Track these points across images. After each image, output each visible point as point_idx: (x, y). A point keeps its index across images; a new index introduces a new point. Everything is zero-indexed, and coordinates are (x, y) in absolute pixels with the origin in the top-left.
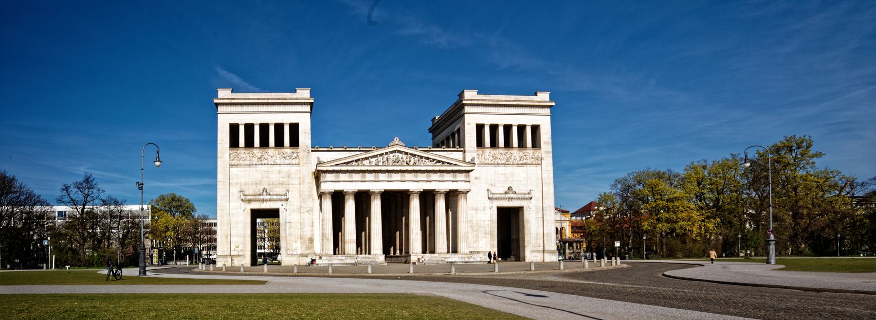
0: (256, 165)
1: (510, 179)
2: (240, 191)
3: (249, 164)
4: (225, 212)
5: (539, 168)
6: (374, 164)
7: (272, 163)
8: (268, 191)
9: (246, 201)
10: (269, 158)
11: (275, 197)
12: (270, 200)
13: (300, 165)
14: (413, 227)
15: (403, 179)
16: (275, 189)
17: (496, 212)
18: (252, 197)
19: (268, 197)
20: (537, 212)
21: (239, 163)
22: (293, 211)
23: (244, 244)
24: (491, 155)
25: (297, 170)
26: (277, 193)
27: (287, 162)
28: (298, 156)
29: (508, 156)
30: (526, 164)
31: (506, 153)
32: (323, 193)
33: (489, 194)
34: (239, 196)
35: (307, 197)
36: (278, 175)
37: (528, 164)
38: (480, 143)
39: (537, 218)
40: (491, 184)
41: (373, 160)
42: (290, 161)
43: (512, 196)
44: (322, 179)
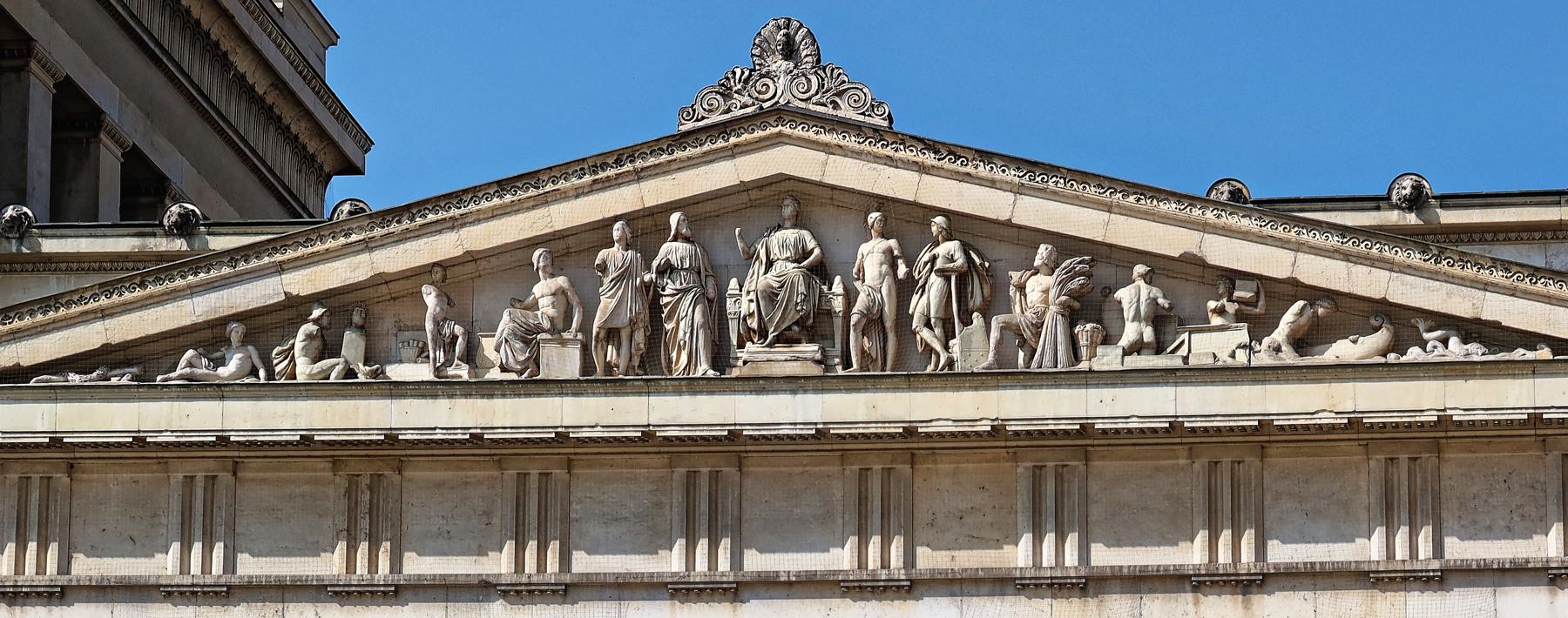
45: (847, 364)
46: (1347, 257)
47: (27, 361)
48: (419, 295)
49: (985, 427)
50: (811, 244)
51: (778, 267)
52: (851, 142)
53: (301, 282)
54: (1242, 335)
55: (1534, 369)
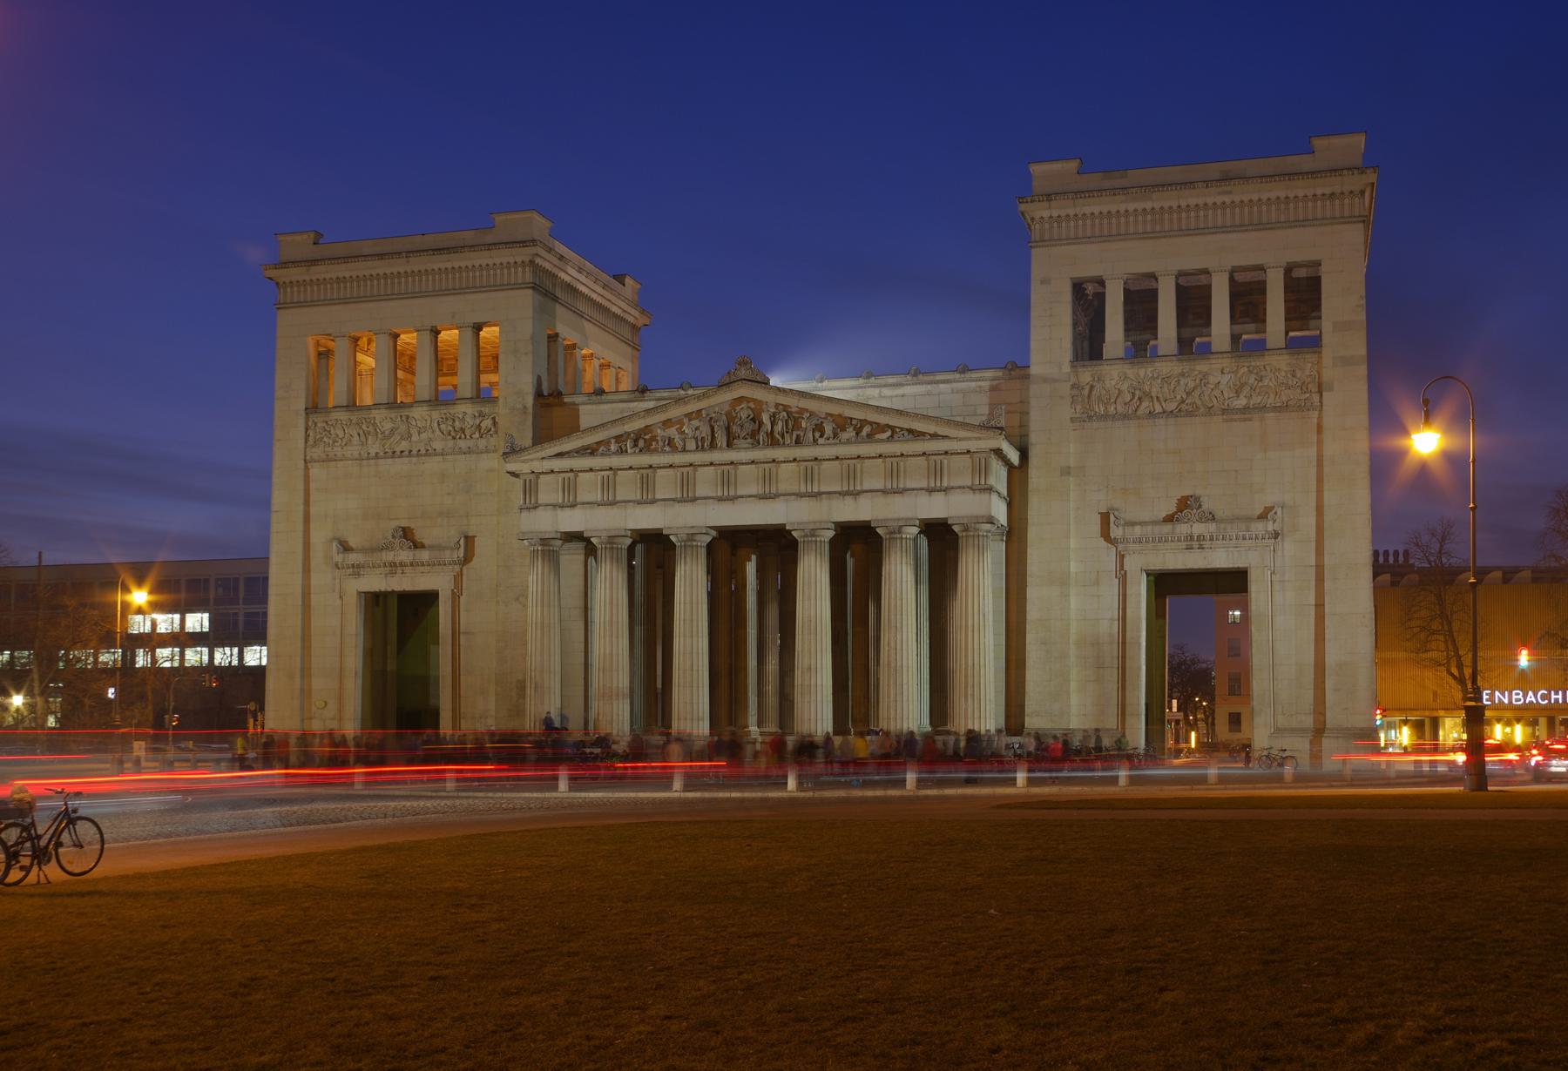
2: (335, 539)
3: (357, 456)
10: (414, 431)
19: (405, 555)
29: (1192, 384)
30: (1262, 408)
31: (1182, 375)
38: (1089, 346)
47: (564, 450)
50: (751, 413)
54: (854, 434)
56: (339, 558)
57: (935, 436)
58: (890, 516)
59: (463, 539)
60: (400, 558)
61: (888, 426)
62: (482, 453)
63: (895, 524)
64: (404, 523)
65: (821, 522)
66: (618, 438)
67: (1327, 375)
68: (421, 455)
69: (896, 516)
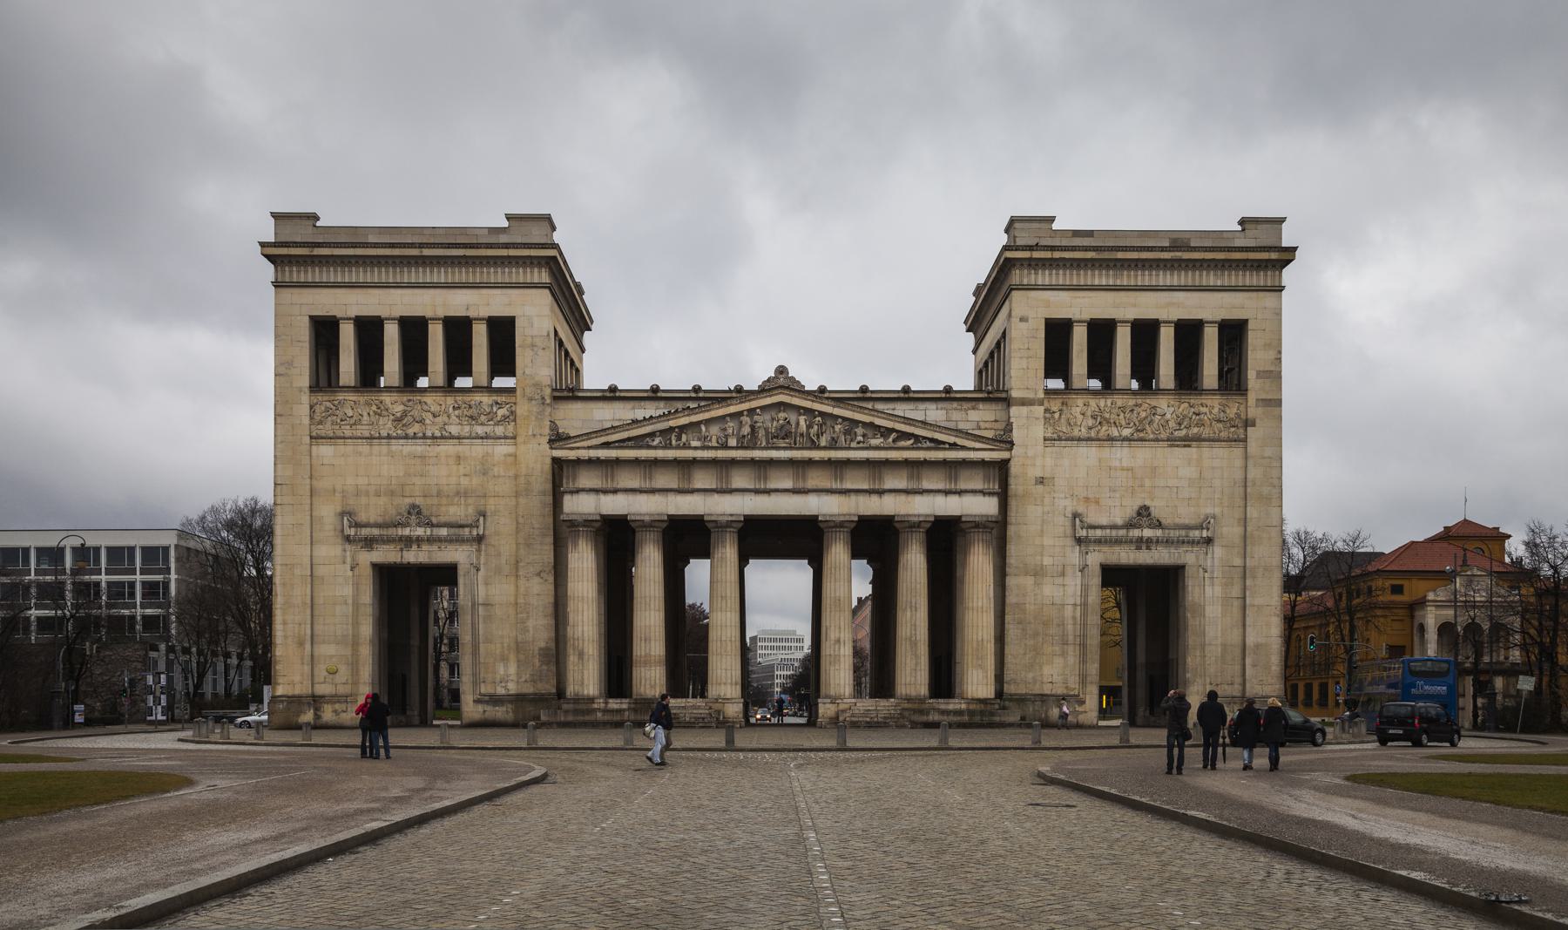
0: (389, 437)
1: (1147, 483)
2: (342, 514)
3: (368, 435)
4: (297, 572)
5: (1238, 452)
6: (716, 445)
7: (438, 434)
8: (425, 512)
9: (360, 540)
10: (428, 418)
11: (444, 532)
12: (431, 540)
13: (519, 439)
14: (828, 624)
15: (800, 485)
16: (443, 509)
17: (1096, 580)
18: (376, 532)
20: (1227, 585)
21: (339, 433)
22: (498, 570)
23: (354, 667)
24: (1089, 413)
25: (510, 455)
26: (452, 519)
27: (480, 430)
28: (512, 412)
29: (1143, 415)
30: (1199, 439)
31: (1136, 405)
32: (572, 524)
33: (1078, 527)
34: (339, 528)
35: (537, 532)
36: (455, 467)
37: (1204, 440)
39: (1226, 600)
40: (1087, 499)
41: (715, 430)
42: (488, 429)
43: (1147, 533)
44: (567, 485)
45: (795, 444)
46: (905, 424)
47: (610, 441)
48: (700, 427)
49: (826, 459)
51: (781, 422)
52: (797, 394)
53: (672, 423)
55: (945, 449)
56: (352, 532)
57: (954, 446)
58: (911, 513)
59: (482, 519)
60: (417, 533)
61: (912, 435)
62: (500, 438)
63: (916, 519)
64: (418, 501)
65: (850, 515)
66: (663, 432)
67: (1253, 412)
68: (436, 438)
69: (916, 512)
